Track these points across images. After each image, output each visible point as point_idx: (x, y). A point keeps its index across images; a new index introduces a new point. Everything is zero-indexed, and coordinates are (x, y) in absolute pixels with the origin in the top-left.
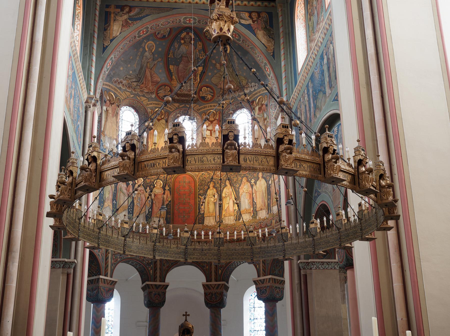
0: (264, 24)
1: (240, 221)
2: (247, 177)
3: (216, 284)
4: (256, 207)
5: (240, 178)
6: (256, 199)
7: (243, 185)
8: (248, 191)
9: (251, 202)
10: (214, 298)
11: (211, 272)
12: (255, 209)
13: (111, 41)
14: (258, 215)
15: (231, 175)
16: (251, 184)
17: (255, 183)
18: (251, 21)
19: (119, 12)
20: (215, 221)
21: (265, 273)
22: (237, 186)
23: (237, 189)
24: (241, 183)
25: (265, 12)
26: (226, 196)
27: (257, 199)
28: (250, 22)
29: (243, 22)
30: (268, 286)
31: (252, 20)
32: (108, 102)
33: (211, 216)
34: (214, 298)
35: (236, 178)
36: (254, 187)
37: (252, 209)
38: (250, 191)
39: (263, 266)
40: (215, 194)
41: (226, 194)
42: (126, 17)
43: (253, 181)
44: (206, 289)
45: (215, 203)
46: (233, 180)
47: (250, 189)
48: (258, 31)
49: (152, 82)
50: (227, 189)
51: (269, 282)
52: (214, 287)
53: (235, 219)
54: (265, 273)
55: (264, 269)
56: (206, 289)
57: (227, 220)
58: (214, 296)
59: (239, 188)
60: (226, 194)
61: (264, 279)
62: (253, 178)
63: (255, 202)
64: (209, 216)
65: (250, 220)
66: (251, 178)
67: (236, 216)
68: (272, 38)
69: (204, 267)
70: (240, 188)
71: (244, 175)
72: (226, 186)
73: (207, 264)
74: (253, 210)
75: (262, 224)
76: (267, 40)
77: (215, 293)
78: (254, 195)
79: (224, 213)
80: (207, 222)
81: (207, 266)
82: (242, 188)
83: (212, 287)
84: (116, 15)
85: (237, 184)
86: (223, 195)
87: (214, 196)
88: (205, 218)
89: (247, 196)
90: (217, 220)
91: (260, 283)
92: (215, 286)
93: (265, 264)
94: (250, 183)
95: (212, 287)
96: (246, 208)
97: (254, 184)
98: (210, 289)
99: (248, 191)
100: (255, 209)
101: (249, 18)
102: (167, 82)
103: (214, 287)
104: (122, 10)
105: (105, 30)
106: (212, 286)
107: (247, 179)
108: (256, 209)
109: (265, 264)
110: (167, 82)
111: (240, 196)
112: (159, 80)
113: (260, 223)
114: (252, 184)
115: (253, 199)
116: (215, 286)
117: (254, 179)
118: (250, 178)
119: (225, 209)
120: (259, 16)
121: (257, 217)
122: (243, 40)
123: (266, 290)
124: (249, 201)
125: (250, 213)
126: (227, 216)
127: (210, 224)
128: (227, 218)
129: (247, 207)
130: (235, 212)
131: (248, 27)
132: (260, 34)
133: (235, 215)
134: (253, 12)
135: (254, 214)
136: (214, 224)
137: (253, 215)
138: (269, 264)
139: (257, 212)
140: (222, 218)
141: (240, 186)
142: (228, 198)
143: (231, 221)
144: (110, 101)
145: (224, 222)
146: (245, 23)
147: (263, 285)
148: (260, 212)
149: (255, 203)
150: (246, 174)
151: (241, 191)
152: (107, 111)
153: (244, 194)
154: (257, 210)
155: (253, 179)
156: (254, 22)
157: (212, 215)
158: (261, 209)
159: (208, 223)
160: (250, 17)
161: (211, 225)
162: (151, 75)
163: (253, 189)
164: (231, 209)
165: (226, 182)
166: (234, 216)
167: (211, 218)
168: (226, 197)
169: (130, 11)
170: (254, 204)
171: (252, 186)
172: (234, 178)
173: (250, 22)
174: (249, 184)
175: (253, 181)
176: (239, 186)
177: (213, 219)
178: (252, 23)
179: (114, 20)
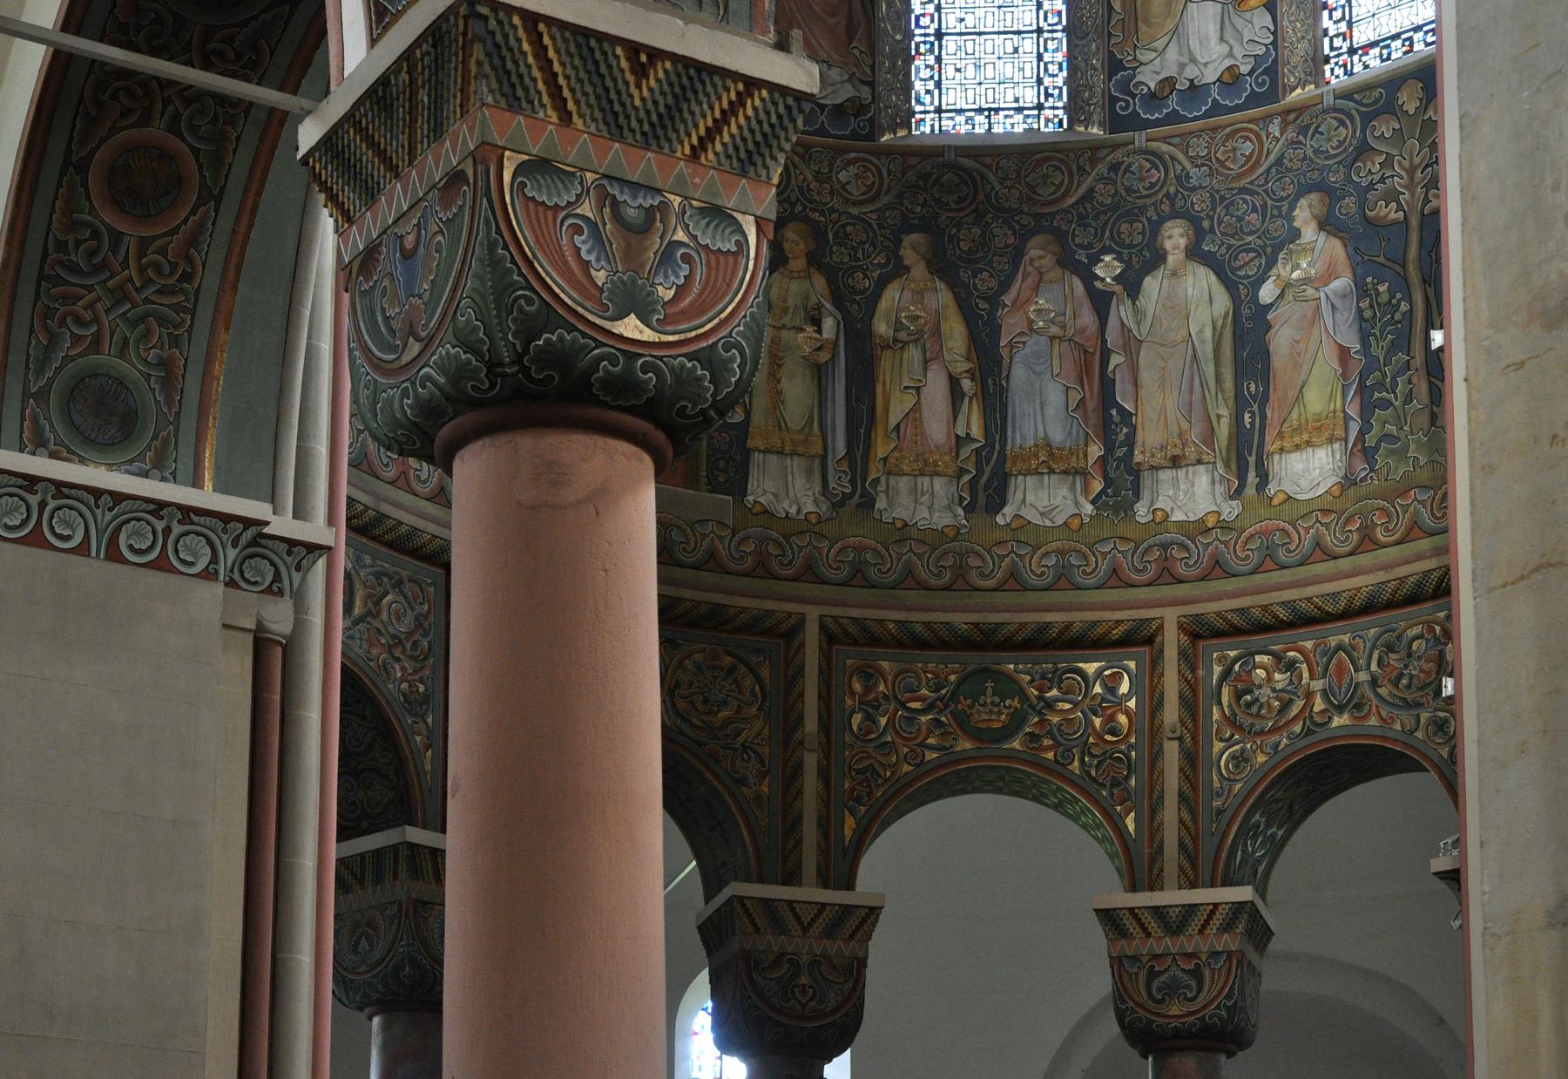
1: (1000, 520)
2: (1060, 236)
3: (823, 906)
4: (1130, 442)
5: (1003, 236)
6: (1130, 388)
7: (1029, 280)
8: (1070, 333)
9: (1091, 404)
10: (804, 992)
11: (793, 826)
12: (1120, 453)
14: (1146, 495)
15: (938, 201)
16: (1092, 292)
17: (1131, 285)
20: (818, 488)
21: (1194, 866)
22: (984, 282)
23: (983, 305)
24: (1014, 272)
26: (903, 335)
27: (1143, 393)
30: (1215, 954)
33: (793, 454)
34: (804, 992)
35: (977, 231)
36: (1122, 311)
37: (1095, 451)
38: (1082, 331)
39: (1181, 821)
40: (819, 306)
41: (898, 320)
43: (1107, 269)
44: (757, 931)
45: (820, 373)
46: (951, 238)
47: (1088, 318)
50: (907, 295)
51: (1228, 927)
52: (813, 920)
53: (961, 499)
54: (1194, 866)
55: (1188, 840)
56: (757, 931)
57: (904, 499)
58: (804, 980)
59: (994, 300)
60: (898, 326)
61: (1191, 909)
62: (1108, 251)
63: (1121, 409)
64: (781, 453)
65: (1077, 521)
66: (1098, 247)
67: (973, 483)
69: (743, 782)
70: (1007, 299)
71: (1038, 217)
72: (899, 270)
73: (762, 763)
74: (1102, 461)
75: (1176, 553)
77: (815, 963)
78: (1115, 360)
79: (881, 449)
80: (770, 486)
81: (762, 776)
82: (1019, 305)
83: (798, 919)
85: (981, 271)
86: (882, 327)
87: (817, 322)
88: (757, 457)
89: (1056, 362)
90: (832, 485)
91: (1152, 925)
92: (817, 916)
93: (1193, 813)
94: (1089, 278)
95: (798, 919)
96: (1046, 437)
97: (1118, 288)
98: (780, 928)
99: (1063, 327)
100: (1120, 453)
103: (813, 920)
106: (796, 915)
107: (1058, 249)
108: (1131, 453)
109: (1193, 813)
111: (1004, 353)
113: (1165, 546)
114: (1098, 284)
115: (1107, 385)
116: (817, 916)
117: (1119, 258)
118: (1081, 246)
119: (893, 422)
121: (1142, 512)
123: (1197, 974)
124: (1075, 397)
125: (1084, 474)
126: (906, 468)
127: (786, 504)
128: (903, 483)
129: (1057, 435)
130: (966, 452)
133: (962, 472)
135: (1108, 481)
136: (811, 508)
137: (1103, 492)
138: (1225, 818)
139: (1136, 472)
140: (872, 476)
141: (1005, 287)
142: (914, 354)
143: (930, 508)
145: (881, 503)
147: (1170, 944)
148: (1164, 475)
149: (1126, 416)
150: (1051, 214)
151: (1011, 325)
153: (1034, 344)
154: (1138, 458)
155: (1107, 258)
157: (800, 450)
158: (1175, 462)
159: (776, 496)
161: (793, 510)
163: (1112, 322)
164: (936, 428)
165: (898, 243)
166: (959, 478)
167: (796, 464)
168: (896, 344)
170: (1117, 419)
171: (1101, 302)
172: (959, 225)
174: (1078, 284)
175: (1107, 269)
176: (994, 283)
177: (809, 473)
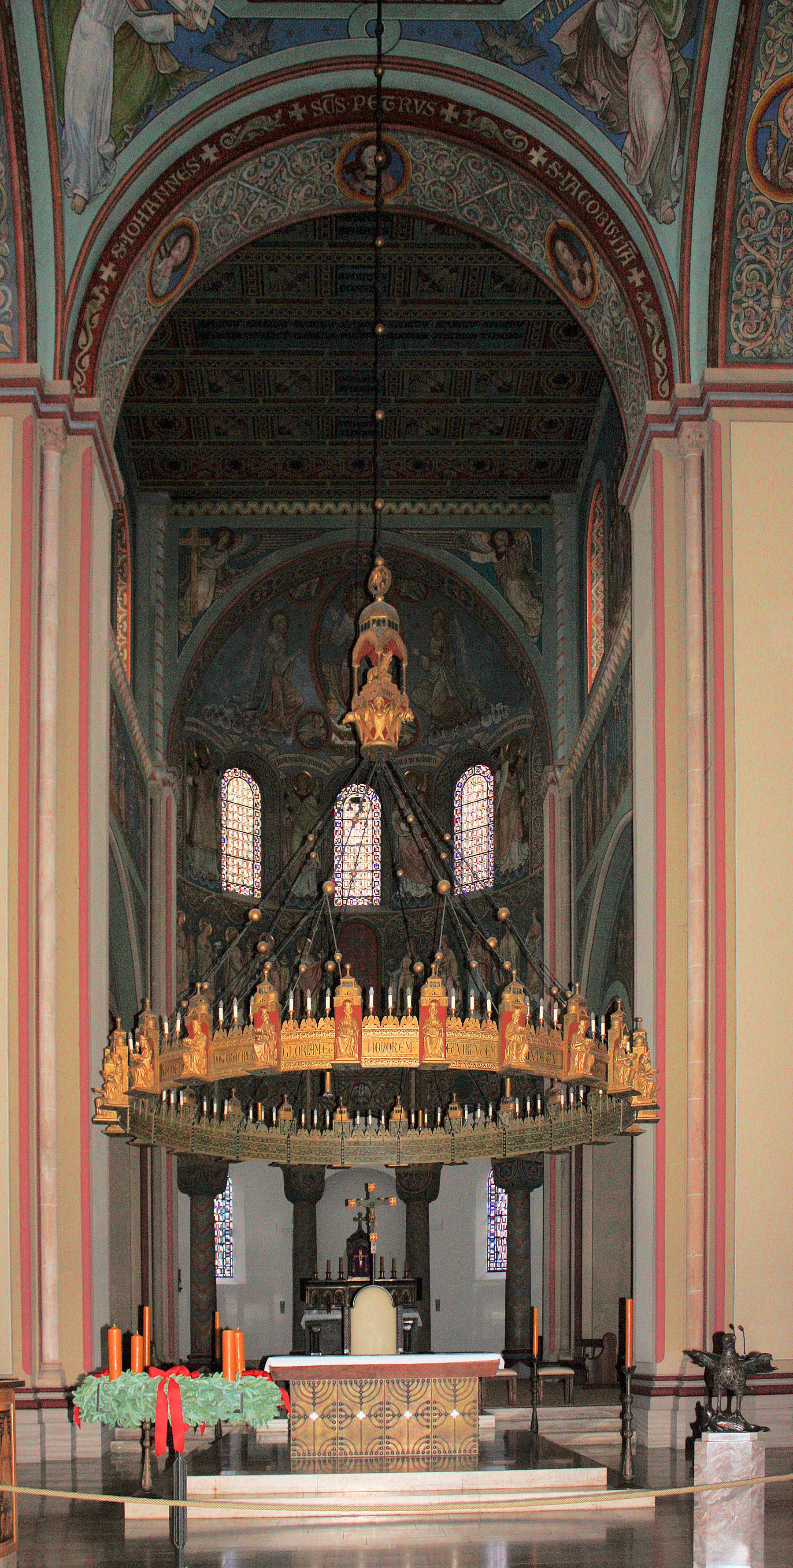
0: (521, 563)
13: (195, 622)
18: (493, 554)
19: (207, 547)
25: (527, 530)
28: (491, 557)
29: (476, 557)
31: (497, 552)
32: (196, 764)
42: (222, 558)
48: (509, 581)
49: (286, 707)
68: (539, 599)
76: (527, 604)
84: (203, 554)
101: (489, 549)
102: (317, 703)
104: (215, 541)
105: (182, 595)
110: (317, 703)
112: (300, 700)
120: (511, 541)
122: (475, 605)
131: (486, 570)
132: (513, 586)
134: (499, 529)
144: (199, 760)
146: (480, 561)
152: (195, 785)
156: (499, 555)
160: (492, 543)
162: (282, 689)
169: (229, 545)
173: (491, 557)
178: (495, 560)
179: (199, 569)
